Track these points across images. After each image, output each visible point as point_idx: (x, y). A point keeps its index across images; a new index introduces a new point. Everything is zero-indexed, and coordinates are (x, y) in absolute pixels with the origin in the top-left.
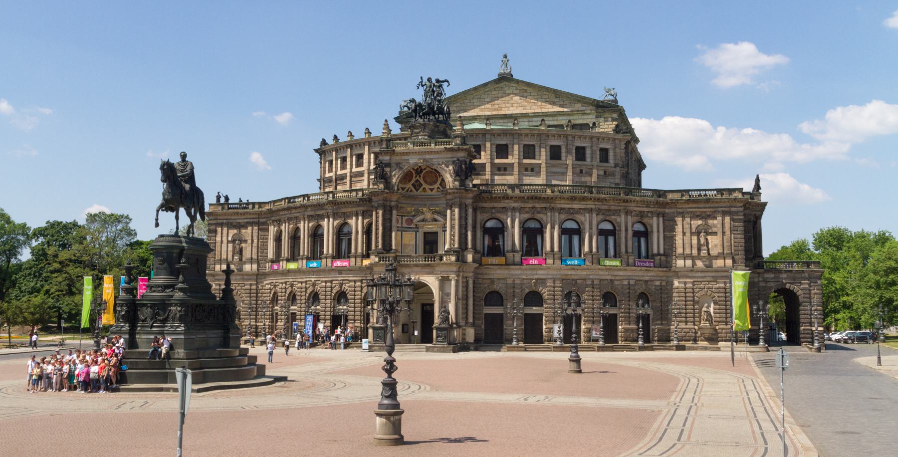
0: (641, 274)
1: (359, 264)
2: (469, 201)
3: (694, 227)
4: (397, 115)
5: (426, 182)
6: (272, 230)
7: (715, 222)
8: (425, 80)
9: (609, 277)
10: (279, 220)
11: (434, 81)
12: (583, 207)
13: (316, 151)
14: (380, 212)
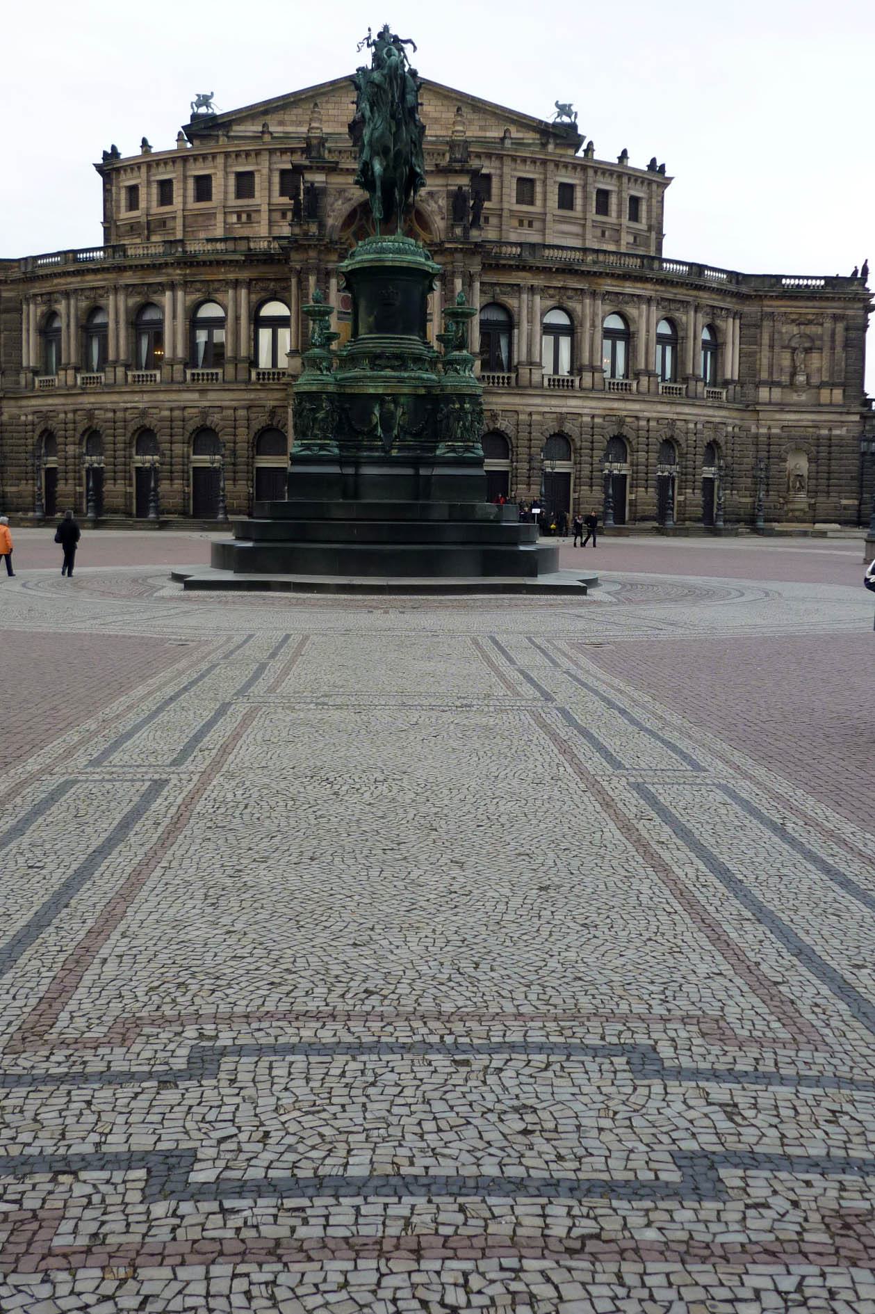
0: (710, 412)
1: (242, 376)
2: (476, 269)
3: (786, 337)
4: (188, 122)
6: (33, 313)
7: (819, 330)
8: (374, 37)
9: (670, 416)
10: (50, 294)
12: (638, 292)
13: (99, 168)
14: (312, 280)
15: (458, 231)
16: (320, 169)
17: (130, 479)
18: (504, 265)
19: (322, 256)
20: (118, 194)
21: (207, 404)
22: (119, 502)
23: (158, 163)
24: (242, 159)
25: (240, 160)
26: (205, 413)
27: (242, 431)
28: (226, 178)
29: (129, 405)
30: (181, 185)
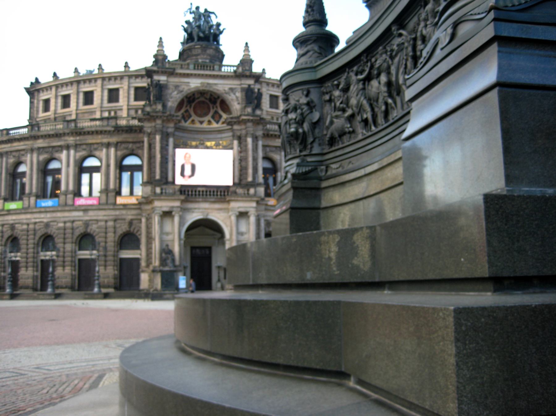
2: (260, 133)
5: (196, 113)
8: (194, 9)
11: (202, 10)
13: (28, 90)
14: (158, 138)
15: (249, 110)
16: (163, 73)
17: (37, 267)
18: (272, 135)
19: (165, 124)
20: (38, 104)
21: (87, 218)
22: (30, 282)
23: (62, 85)
24: (112, 82)
25: (111, 82)
26: (87, 224)
27: (111, 236)
28: (102, 91)
29: (37, 220)
30: (76, 96)
